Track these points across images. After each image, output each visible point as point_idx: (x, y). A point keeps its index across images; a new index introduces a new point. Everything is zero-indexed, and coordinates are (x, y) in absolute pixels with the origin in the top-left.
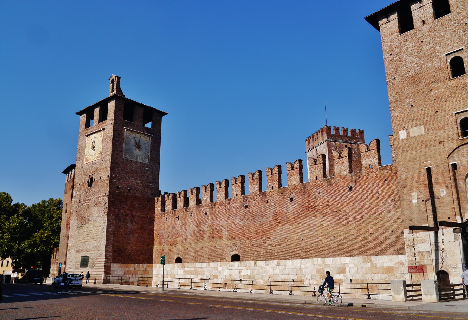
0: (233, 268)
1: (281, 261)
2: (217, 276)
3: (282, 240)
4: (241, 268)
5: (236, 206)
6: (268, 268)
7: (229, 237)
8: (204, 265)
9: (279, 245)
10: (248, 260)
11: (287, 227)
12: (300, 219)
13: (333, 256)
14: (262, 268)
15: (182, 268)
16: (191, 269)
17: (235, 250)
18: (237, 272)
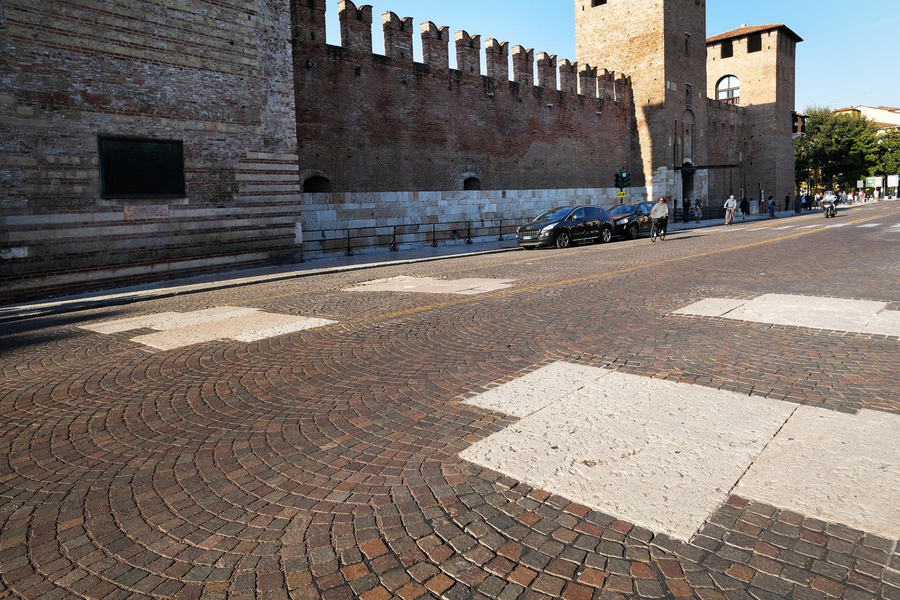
0: (469, 201)
1: (536, 190)
2: (437, 218)
3: (537, 162)
4: (482, 202)
5: (470, 89)
6: (521, 200)
7: (458, 145)
8: (404, 197)
9: (534, 168)
10: (492, 189)
11: (543, 144)
12: (556, 138)
13: (583, 187)
14: (513, 201)
15: (331, 205)
16: (364, 206)
17: (471, 170)
18: (476, 208)
